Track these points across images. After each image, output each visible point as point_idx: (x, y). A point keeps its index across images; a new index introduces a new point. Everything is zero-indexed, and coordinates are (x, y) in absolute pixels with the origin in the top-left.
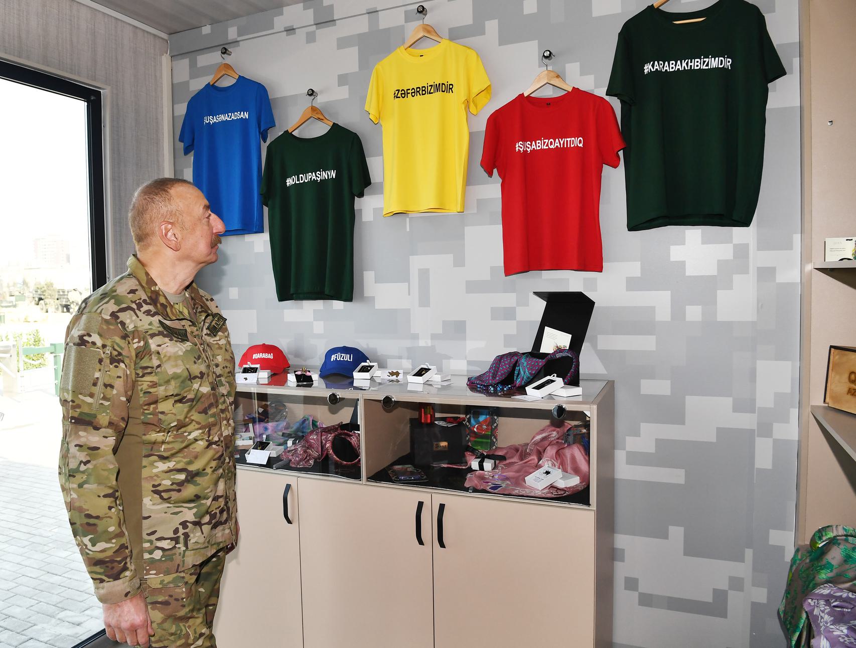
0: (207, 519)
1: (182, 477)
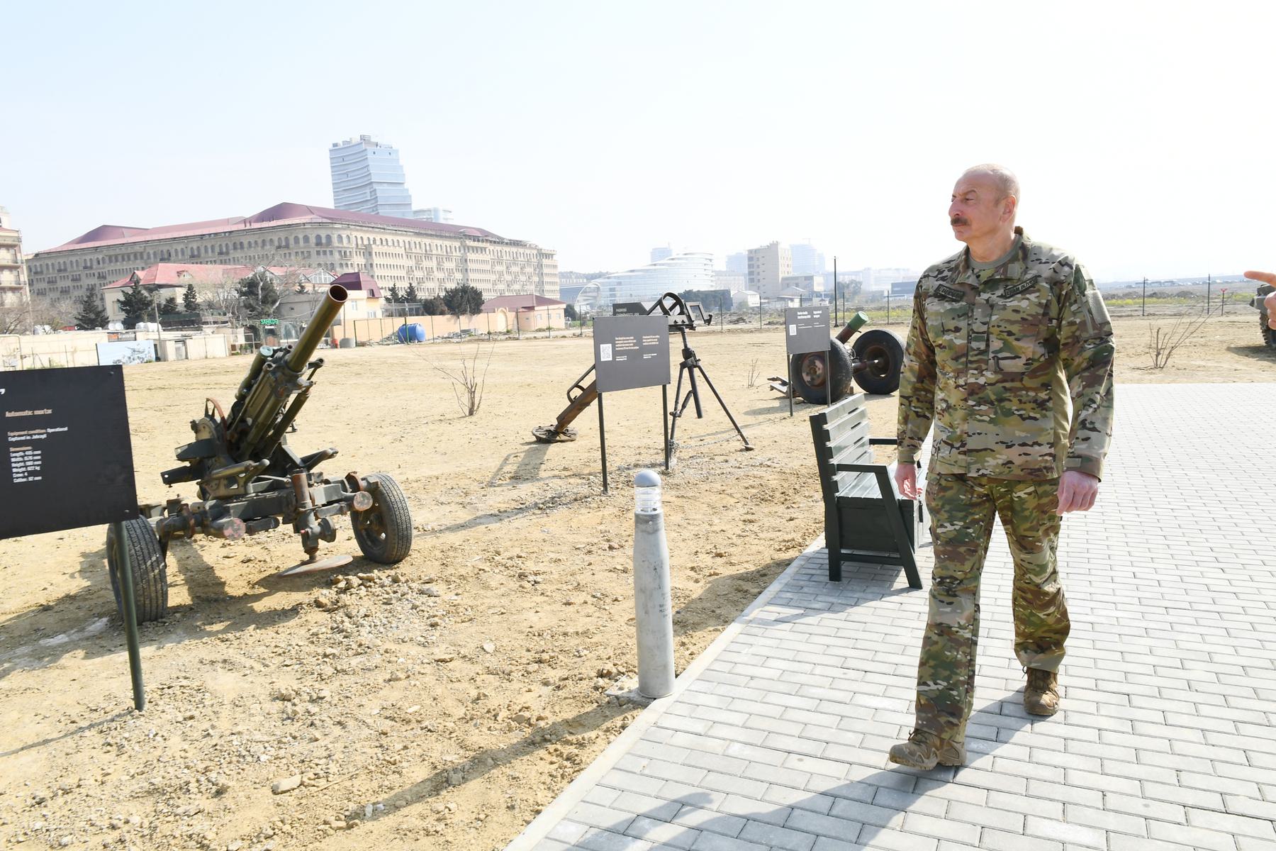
0: (957, 445)
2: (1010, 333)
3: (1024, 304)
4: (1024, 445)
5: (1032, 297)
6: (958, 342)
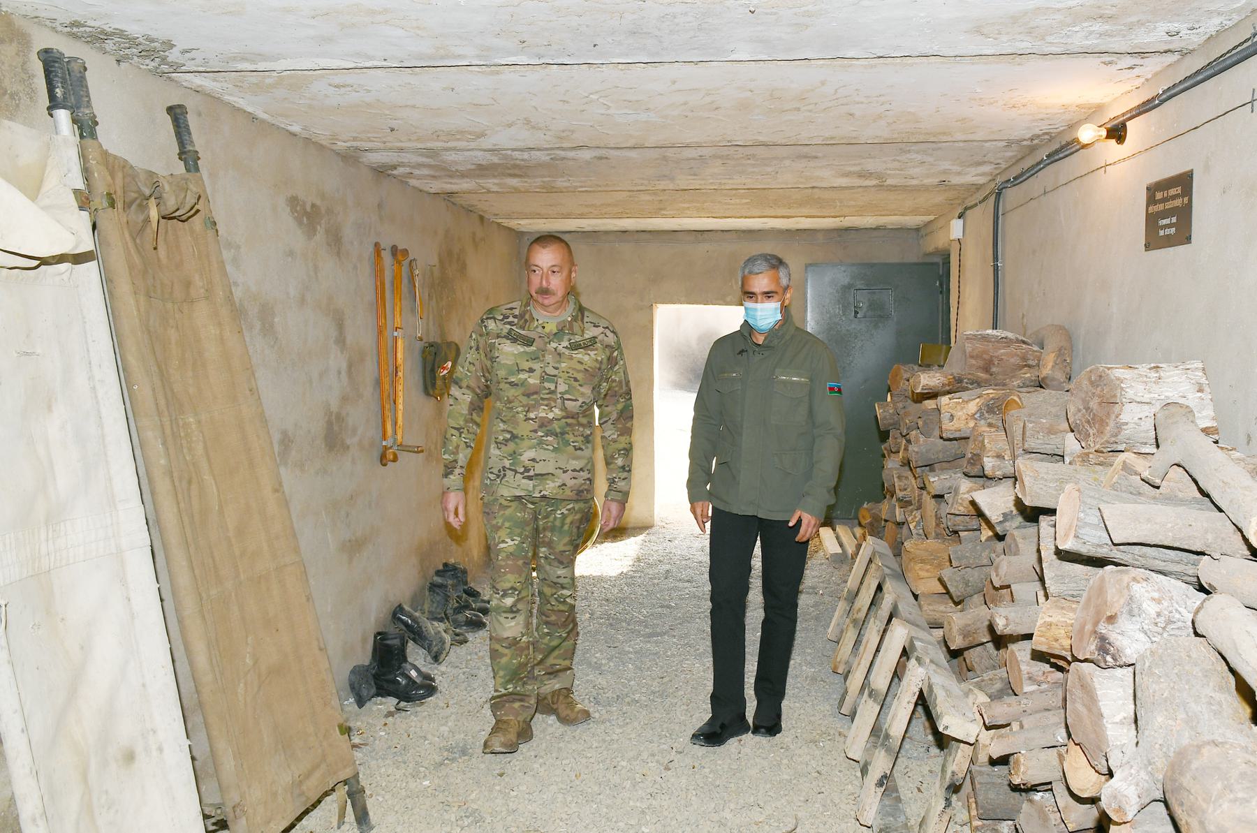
0: (522, 470)
1: (508, 436)
2: (576, 380)
3: (586, 358)
4: (574, 470)
5: (592, 353)
6: (531, 381)
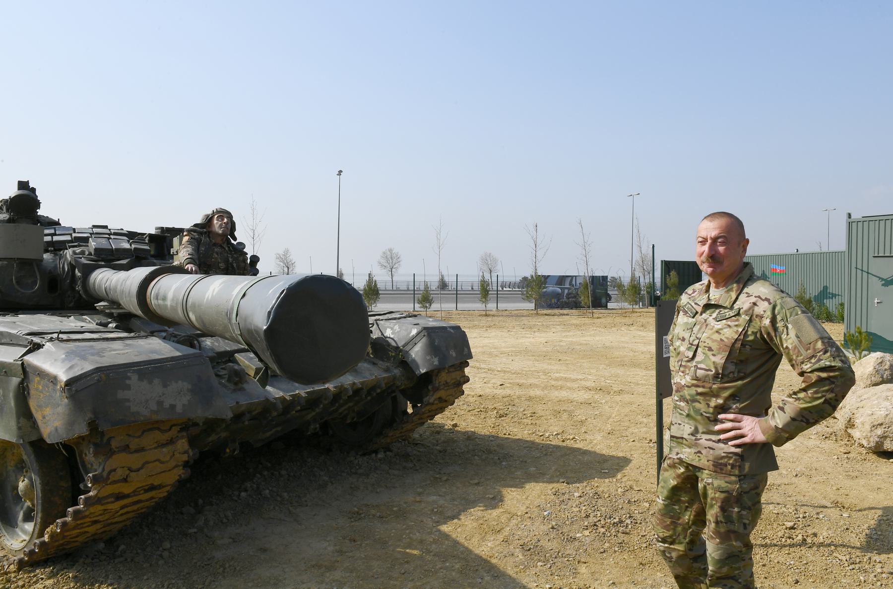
2: (710, 349)
